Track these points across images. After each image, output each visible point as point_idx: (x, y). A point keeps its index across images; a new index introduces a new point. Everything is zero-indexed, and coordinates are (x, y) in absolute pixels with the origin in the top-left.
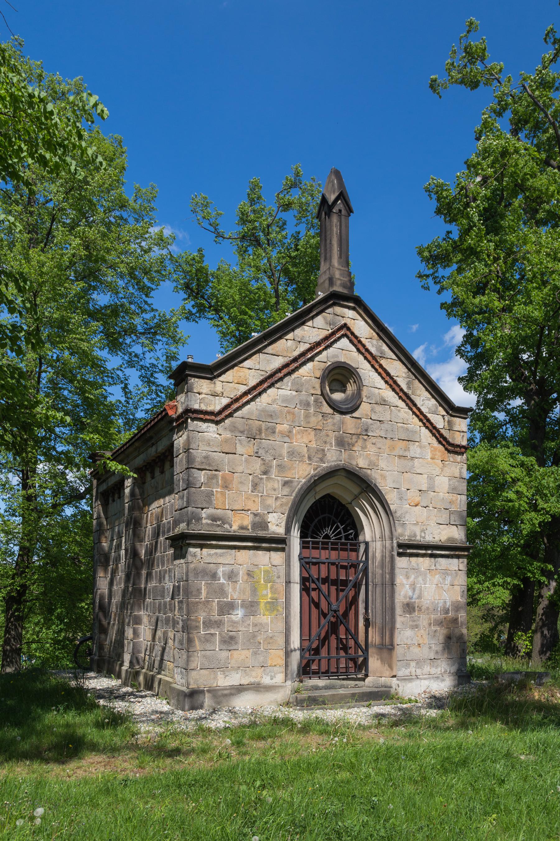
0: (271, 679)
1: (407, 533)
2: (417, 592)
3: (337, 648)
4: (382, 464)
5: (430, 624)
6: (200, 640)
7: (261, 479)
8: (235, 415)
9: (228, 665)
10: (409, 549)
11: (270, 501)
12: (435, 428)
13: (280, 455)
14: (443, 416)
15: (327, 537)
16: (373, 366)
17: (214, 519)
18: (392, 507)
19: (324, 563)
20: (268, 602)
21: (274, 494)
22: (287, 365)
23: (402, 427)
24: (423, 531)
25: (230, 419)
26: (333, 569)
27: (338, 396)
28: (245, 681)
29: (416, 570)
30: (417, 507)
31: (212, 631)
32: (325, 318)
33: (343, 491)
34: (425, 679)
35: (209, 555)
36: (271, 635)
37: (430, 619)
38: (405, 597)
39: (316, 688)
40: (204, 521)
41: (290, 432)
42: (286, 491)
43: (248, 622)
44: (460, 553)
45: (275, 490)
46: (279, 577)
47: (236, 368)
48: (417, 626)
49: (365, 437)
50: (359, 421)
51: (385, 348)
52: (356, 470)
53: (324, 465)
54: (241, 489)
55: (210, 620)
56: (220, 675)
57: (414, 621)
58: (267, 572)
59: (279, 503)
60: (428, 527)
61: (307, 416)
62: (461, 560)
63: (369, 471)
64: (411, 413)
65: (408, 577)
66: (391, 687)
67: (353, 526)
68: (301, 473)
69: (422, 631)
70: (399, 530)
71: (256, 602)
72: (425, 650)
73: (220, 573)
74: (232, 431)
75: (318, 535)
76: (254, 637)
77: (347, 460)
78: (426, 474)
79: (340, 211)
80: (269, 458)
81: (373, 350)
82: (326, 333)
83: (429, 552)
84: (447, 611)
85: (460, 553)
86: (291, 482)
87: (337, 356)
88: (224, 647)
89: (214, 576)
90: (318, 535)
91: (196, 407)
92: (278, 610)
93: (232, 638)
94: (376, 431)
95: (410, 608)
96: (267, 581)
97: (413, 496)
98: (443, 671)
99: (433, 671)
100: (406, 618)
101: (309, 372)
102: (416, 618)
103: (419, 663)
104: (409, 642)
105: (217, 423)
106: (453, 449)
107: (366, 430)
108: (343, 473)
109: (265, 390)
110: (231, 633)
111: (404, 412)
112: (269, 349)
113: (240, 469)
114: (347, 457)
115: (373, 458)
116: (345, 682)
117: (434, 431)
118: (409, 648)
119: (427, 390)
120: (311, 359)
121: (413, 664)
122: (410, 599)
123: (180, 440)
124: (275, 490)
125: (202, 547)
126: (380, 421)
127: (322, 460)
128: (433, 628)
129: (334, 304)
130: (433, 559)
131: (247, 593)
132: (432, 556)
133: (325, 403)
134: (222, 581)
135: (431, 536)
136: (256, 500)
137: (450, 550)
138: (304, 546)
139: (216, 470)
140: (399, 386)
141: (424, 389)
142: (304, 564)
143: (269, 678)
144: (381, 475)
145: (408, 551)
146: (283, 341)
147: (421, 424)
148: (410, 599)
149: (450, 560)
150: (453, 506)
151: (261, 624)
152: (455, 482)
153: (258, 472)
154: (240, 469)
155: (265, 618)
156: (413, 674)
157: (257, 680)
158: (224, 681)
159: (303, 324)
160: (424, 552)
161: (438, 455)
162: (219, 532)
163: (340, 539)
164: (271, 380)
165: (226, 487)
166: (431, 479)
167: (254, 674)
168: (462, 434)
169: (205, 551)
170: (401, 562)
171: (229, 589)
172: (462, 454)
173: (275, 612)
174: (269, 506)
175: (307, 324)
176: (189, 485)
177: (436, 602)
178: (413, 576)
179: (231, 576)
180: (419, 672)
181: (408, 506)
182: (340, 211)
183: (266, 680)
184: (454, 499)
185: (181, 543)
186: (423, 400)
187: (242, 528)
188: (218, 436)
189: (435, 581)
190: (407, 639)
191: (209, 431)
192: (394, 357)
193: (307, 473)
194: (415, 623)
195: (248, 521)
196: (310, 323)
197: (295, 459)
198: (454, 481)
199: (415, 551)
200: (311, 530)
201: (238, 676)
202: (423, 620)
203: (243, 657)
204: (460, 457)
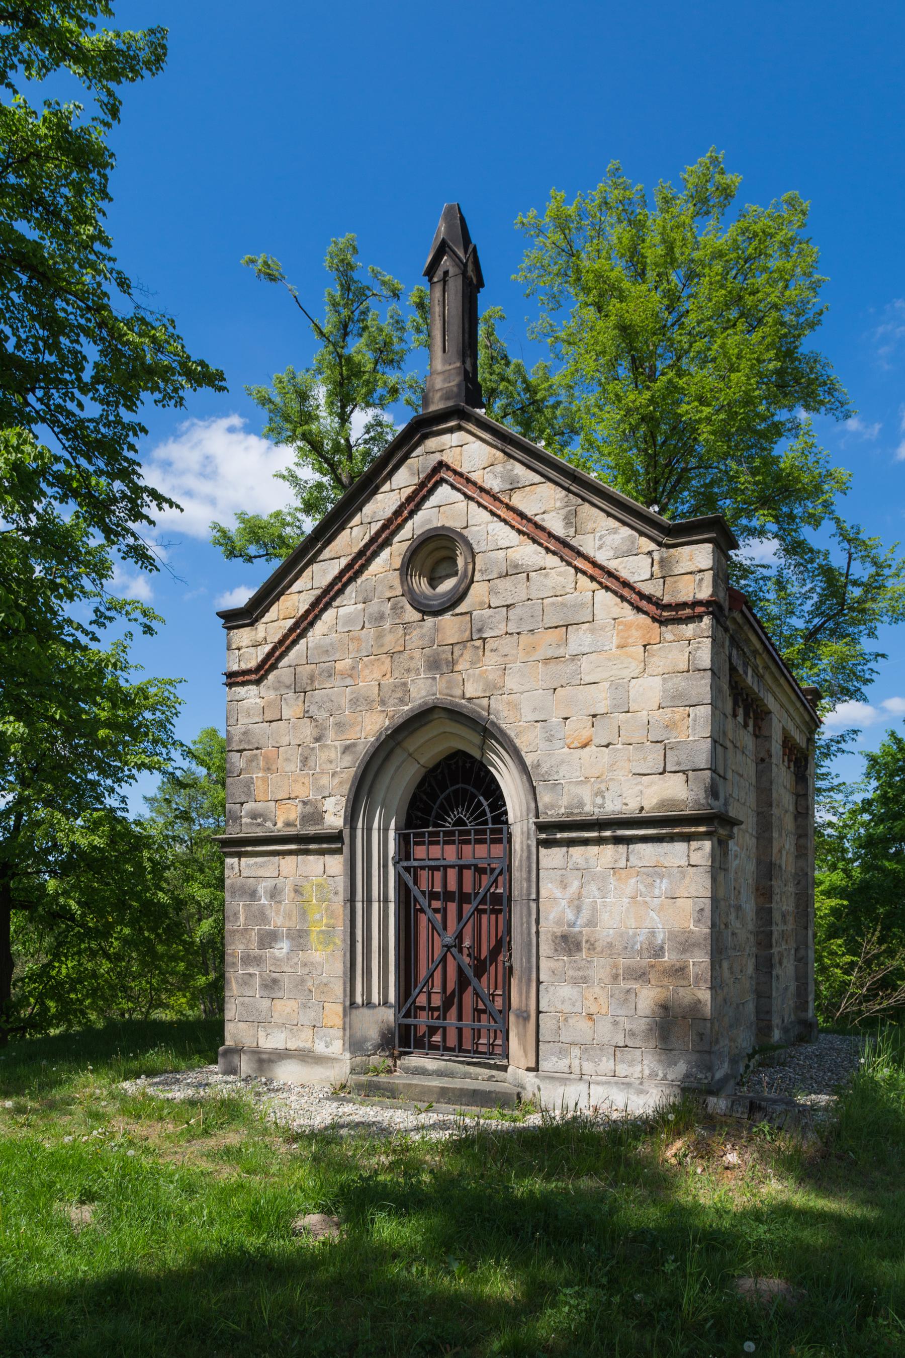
0: (327, 1047)
1: (564, 801)
2: (585, 915)
3: (476, 1010)
4: (511, 683)
5: (615, 977)
6: (237, 982)
7: (313, 749)
8: (280, 665)
9: (270, 1020)
10: (555, 832)
11: (325, 780)
12: (626, 584)
13: (339, 708)
14: (650, 553)
15: (460, 822)
16: (493, 514)
17: (254, 816)
18: (529, 760)
19: (453, 867)
20: (321, 931)
21: (330, 768)
22: (349, 566)
23: (553, 604)
25: (275, 672)
26: (468, 874)
28: (292, 1045)
29: (583, 872)
30: (587, 749)
31: (251, 970)
32: (410, 469)
33: (468, 742)
34: (598, 1083)
35: (248, 866)
36: (325, 981)
38: (559, 922)
39: (423, 1072)
40: (244, 820)
41: (353, 668)
42: (347, 760)
43: (296, 960)
44: (687, 830)
45: (331, 762)
46: (336, 893)
47: (282, 598)
48: (585, 980)
49: (479, 643)
50: (467, 617)
52: (461, 705)
53: (406, 708)
54: (287, 769)
55: (249, 956)
56: (261, 1034)
57: (579, 969)
58: (319, 886)
59: (336, 780)
60: (612, 785)
61: (379, 637)
62: (694, 844)
63: (485, 702)
64: (572, 571)
65: (564, 885)
66: (524, 1089)
68: (368, 728)
69: (597, 990)
70: (545, 798)
71: (306, 931)
73: (261, 891)
74: (276, 689)
75: (446, 821)
76: (303, 981)
77: (445, 691)
78: (606, 680)
79: (446, 273)
80: (321, 715)
81: (494, 483)
82: (409, 490)
83: (608, 833)
84: (658, 952)
85: (687, 830)
86: (354, 745)
87: (430, 521)
88: (265, 994)
90: (446, 821)
91: (235, 668)
92: (335, 943)
93: (275, 981)
95: (569, 943)
96: (321, 900)
97: (579, 728)
98: (647, 1072)
99: (622, 1069)
100: (561, 964)
102: (583, 964)
103: (588, 1048)
104: (567, 1008)
105: (258, 682)
107: (480, 630)
108: (443, 714)
109: (317, 617)
110: (274, 975)
111: (559, 574)
112: (326, 554)
113: (285, 741)
114: (444, 685)
115: (493, 676)
116: (472, 1069)
117: (626, 592)
118: (566, 1020)
119: (609, 515)
120: (387, 543)
121: (576, 1051)
122: (569, 926)
124: (331, 762)
125: (240, 855)
126: (508, 606)
127: (402, 701)
128: (624, 985)
129: (425, 437)
130: (622, 848)
131: (294, 919)
132: (618, 840)
133: (408, 606)
134: (263, 901)
136: (306, 781)
137: (666, 826)
139: (257, 749)
140: (542, 529)
141: (602, 514)
142: (402, 871)
143: (323, 1044)
144: (509, 703)
145: (559, 836)
146: (346, 533)
147: (595, 585)
148: (569, 926)
149: (666, 847)
150: (674, 733)
151: (312, 963)
152: (679, 682)
153: (309, 739)
154: (285, 741)
155: (317, 955)
156: (576, 1070)
157: (308, 1045)
158: (271, 1041)
159: (375, 492)
160: (595, 834)
161: (636, 637)
162: (260, 833)
163: (485, 823)
165: (269, 769)
166: (619, 687)
167: (303, 1035)
169: (244, 860)
170: (552, 857)
171: (271, 914)
172: (700, 617)
173: (331, 947)
174: (323, 787)
175: (382, 490)
177: (631, 932)
178: (576, 884)
179: (274, 894)
180: (588, 1067)
181: (566, 750)
182: (446, 273)
183: (320, 1048)
184: (677, 717)
186: (601, 538)
187: (288, 824)
188: (258, 700)
189: (629, 890)
190: (563, 1002)
192: (537, 478)
193: (378, 727)
194: (581, 973)
196: (386, 487)
197: (359, 708)
199: (574, 835)
200: (433, 813)
201: (283, 1036)
202: (600, 968)
203: (288, 1010)
204: (691, 626)
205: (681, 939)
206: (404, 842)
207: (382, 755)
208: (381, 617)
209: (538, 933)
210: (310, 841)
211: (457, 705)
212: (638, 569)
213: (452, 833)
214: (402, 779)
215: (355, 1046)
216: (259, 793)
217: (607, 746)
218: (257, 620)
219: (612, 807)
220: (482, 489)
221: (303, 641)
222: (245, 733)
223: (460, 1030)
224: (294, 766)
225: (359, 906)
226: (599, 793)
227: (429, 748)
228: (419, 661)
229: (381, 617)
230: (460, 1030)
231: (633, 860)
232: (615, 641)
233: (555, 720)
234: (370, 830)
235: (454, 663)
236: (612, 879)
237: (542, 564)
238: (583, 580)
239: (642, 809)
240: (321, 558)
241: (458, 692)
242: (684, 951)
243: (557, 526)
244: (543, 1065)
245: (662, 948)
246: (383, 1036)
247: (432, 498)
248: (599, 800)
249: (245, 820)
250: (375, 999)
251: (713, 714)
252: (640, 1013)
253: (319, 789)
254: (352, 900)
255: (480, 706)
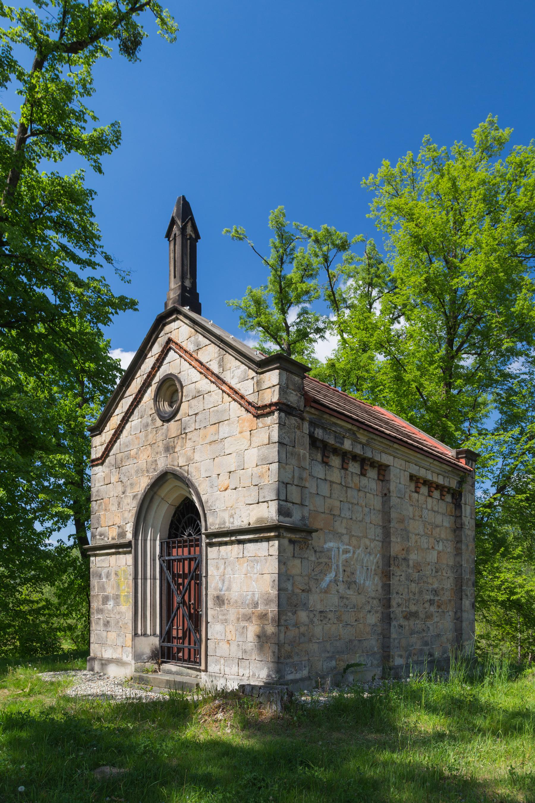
2: (226, 583)
4: (197, 457)
5: (238, 619)
22: (135, 399)
24: (232, 516)
30: (227, 491)
31: (99, 616)
32: (159, 344)
37: (238, 613)
38: (215, 589)
39: (169, 672)
44: (266, 535)
48: (226, 621)
50: (180, 422)
51: (201, 338)
57: (224, 615)
58: (124, 571)
60: (237, 511)
61: (146, 436)
64: (221, 391)
69: (231, 627)
72: (234, 648)
73: (103, 575)
74: (109, 467)
76: (118, 622)
77: (171, 463)
81: (190, 347)
83: (233, 538)
85: (266, 535)
86: (137, 495)
87: (166, 371)
89: (100, 576)
93: (108, 622)
100: (216, 612)
106: (260, 411)
107: (184, 429)
108: (171, 476)
111: (216, 394)
115: (190, 453)
119: (236, 359)
120: (150, 385)
121: (222, 661)
125: (96, 555)
126: (196, 414)
128: (243, 624)
129: (164, 325)
130: (241, 546)
132: (240, 542)
133: (157, 418)
135: (240, 520)
145: (214, 540)
147: (230, 399)
149: (259, 545)
153: (121, 493)
158: (108, 654)
159: (145, 358)
162: (102, 543)
168: (273, 389)
170: (213, 552)
177: (245, 593)
178: (223, 567)
179: (108, 575)
181: (219, 492)
188: (102, 474)
189: (244, 571)
192: (208, 342)
194: (224, 617)
198: (263, 450)
204: (270, 418)
205: (265, 597)
206: (167, 546)
207: (148, 499)
208: (147, 425)
209: (206, 595)
210: (120, 548)
211: (175, 470)
212: (247, 389)
213: (185, 541)
214: (162, 514)
215: (137, 657)
216: (102, 523)
217: (235, 489)
218: (102, 431)
220: (186, 352)
221: (118, 441)
222: (97, 491)
223: (190, 650)
224: (114, 508)
225: (140, 581)
226: (232, 516)
227: (170, 496)
228: (161, 449)
229: (147, 425)
230: (190, 650)
231: (246, 554)
232: (239, 429)
233: (214, 476)
234: (145, 540)
235: (174, 447)
236: (237, 564)
237: (209, 390)
238: (225, 396)
239: (249, 524)
240: (125, 396)
241: (176, 464)
242: (267, 604)
243: (214, 367)
244: (210, 669)
245: (258, 603)
246: (153, 652)
247: (167, 358)
248: (232, 520)
249: (98, 537)
250: (148, 632)
251: (279, 468)
252: (249, 640)
253: (124, 519)
254: (136, 578)
255: (184, 470)
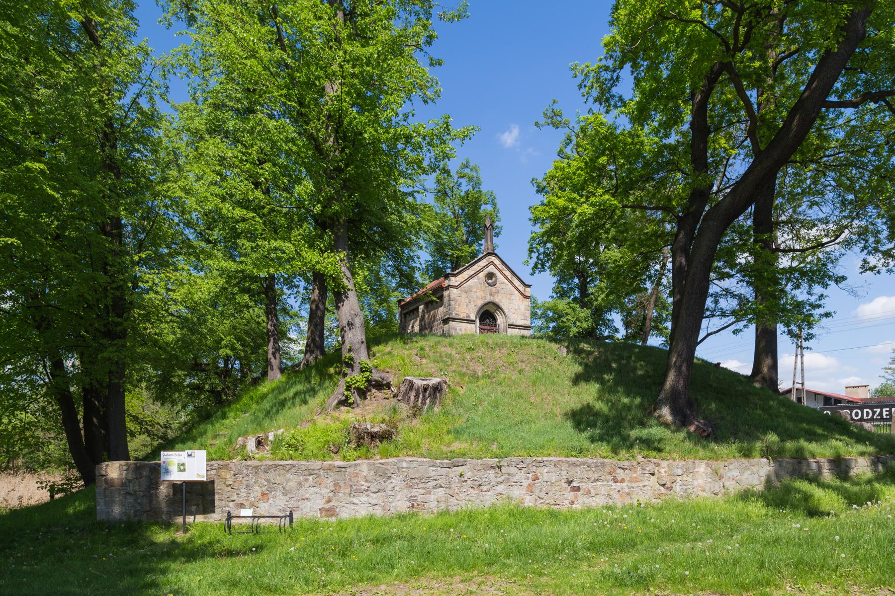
10: (511, 326)
27: (490, 281)
33: (491, 309)
67: (494, 319)
94: (501, 291)
97: (513, 310)
101: (482, 275)
123: (446, 293)
138: (480, 324)
164: (471, 277)
176: (449, 305)
185: (446, 321)
191: (455, 290)
195: (465, 315)
219: (518, 324)
